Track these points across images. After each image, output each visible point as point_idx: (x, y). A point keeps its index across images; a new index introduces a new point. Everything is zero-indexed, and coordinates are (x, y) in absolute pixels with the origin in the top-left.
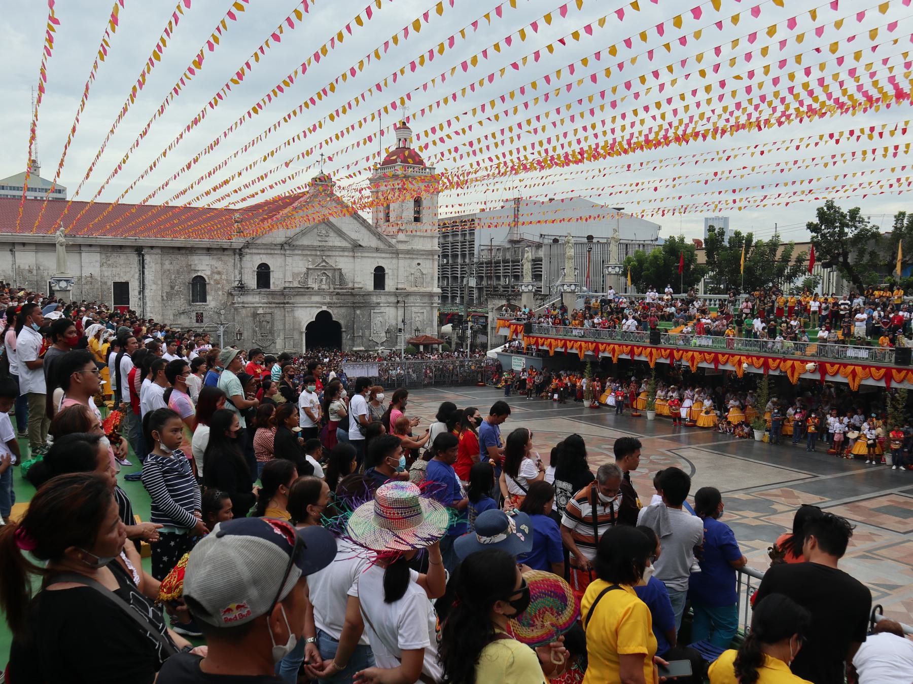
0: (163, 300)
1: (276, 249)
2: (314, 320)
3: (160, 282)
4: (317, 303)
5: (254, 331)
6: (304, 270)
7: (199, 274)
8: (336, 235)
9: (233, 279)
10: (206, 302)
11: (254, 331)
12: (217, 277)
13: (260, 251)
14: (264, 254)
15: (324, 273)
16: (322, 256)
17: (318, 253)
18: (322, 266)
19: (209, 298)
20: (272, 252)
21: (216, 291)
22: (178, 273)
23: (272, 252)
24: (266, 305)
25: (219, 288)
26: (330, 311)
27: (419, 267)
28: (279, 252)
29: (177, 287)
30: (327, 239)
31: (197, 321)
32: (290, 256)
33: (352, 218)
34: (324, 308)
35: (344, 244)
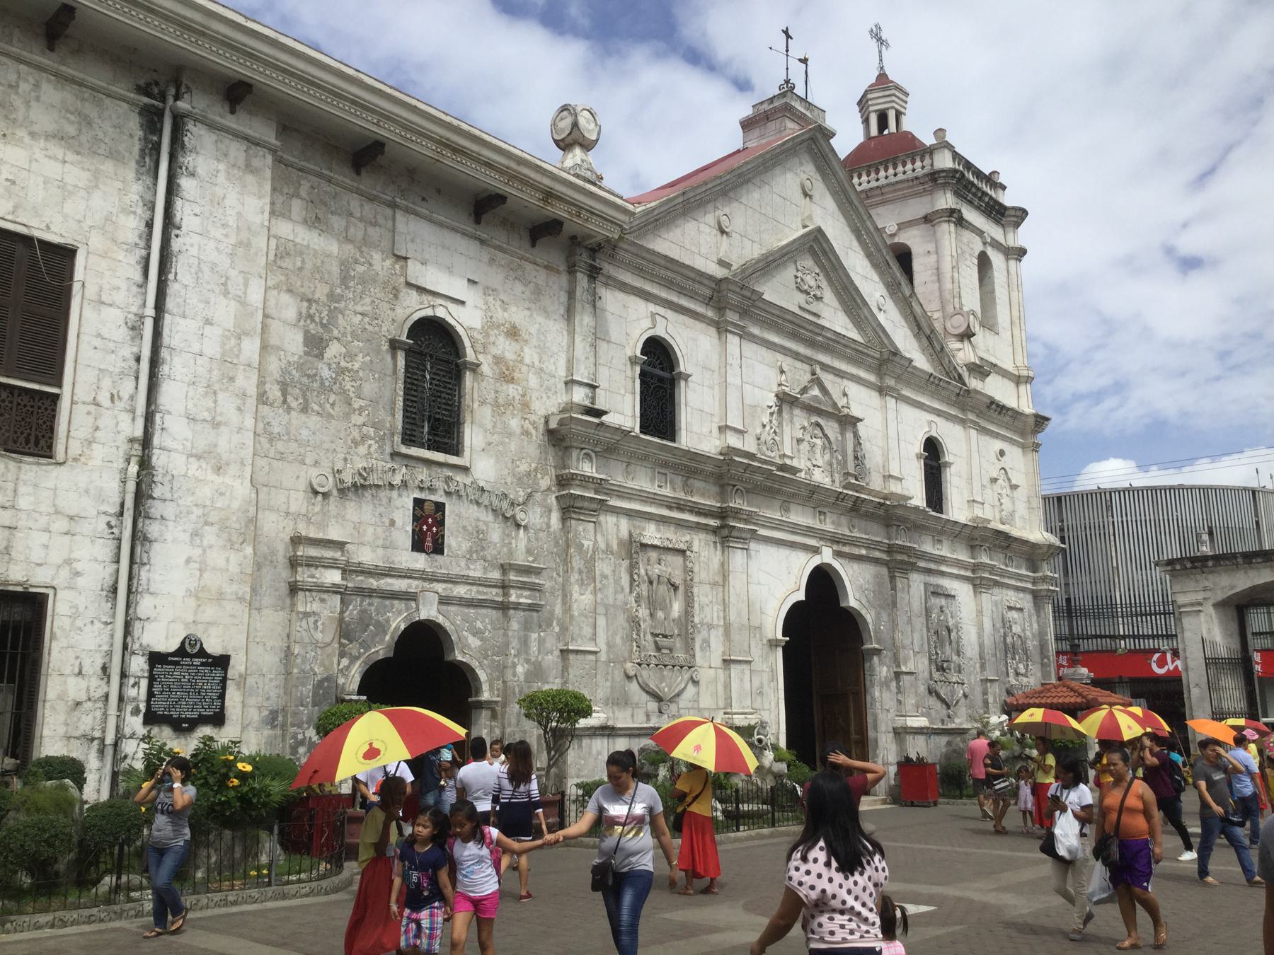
0: (262, 398)
1: (692, 296)
2: (803, 598)
3: (255, 295)
4: (809, 531)
5: (635, 623)
6: (772, 400)
7: (441, 313)
8: (836, 304)
9: (562, 372)
10: (456, 450)
11: (635, 623)
12: (505, 347)
13: (649, 287)
15: (818, 425)
17: (802, 349)
19: (472, 436)
20: (684, 302)
21: (500, 408)
22: (345, 279)
23: (684, 302)
24: (665, 512)
25: (509, 404)
26: (837, 565)
29: (334, 350)
31: (418, 546)
33: (866, 263)
34: (827, 556)
35: (854, 334)
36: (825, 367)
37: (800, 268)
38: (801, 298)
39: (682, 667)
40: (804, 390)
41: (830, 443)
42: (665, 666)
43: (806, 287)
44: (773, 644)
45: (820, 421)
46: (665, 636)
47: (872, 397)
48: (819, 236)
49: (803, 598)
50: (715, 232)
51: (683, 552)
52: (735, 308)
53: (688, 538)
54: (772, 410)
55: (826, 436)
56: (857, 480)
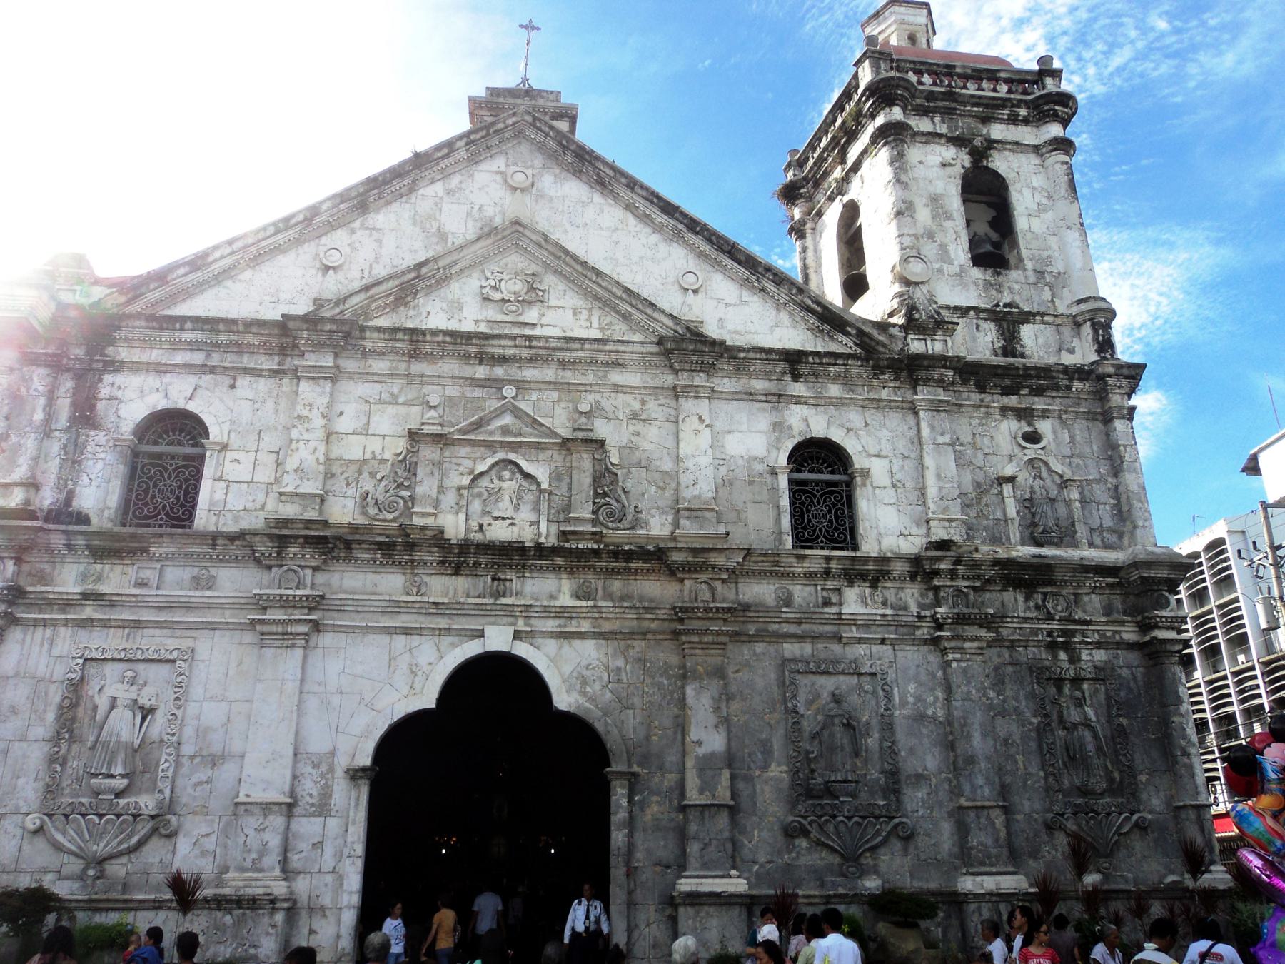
2: (431, 704)
6: (401, 445)
14: (188, 369)
16: (497, 384)
18: (505, 430)
26: (522, 650)
27: (1032, 451)
28: (271, 363)
30: (531, 315)
32: (316, 376)
34: (498, 639)
36: (522, 385)
37: (489, 275)
38: (492, 313)
39: (135, 816)
40: (478, 425)
41: (538, 484)
42: (101, 816)
43: (498, 296)
44: (355, 775)
45: (512, 456)
46: (112, 776)
47: (655, 408)
48: (521, 229)
49: (431, 704)
50: (314, 272)
51: (174, 661)
52: (317, 347)
53: (190, 643)
54: (400, 458)
55: (527, 476)
56: (594, 522)
